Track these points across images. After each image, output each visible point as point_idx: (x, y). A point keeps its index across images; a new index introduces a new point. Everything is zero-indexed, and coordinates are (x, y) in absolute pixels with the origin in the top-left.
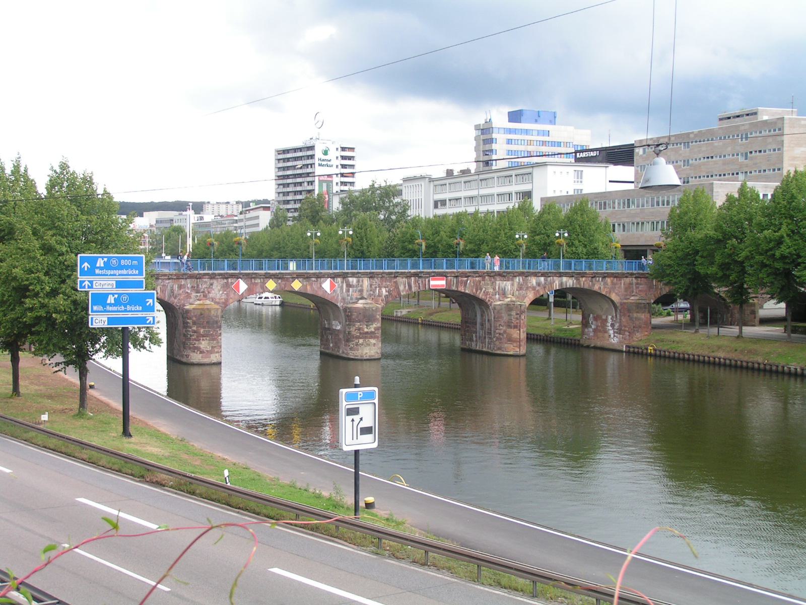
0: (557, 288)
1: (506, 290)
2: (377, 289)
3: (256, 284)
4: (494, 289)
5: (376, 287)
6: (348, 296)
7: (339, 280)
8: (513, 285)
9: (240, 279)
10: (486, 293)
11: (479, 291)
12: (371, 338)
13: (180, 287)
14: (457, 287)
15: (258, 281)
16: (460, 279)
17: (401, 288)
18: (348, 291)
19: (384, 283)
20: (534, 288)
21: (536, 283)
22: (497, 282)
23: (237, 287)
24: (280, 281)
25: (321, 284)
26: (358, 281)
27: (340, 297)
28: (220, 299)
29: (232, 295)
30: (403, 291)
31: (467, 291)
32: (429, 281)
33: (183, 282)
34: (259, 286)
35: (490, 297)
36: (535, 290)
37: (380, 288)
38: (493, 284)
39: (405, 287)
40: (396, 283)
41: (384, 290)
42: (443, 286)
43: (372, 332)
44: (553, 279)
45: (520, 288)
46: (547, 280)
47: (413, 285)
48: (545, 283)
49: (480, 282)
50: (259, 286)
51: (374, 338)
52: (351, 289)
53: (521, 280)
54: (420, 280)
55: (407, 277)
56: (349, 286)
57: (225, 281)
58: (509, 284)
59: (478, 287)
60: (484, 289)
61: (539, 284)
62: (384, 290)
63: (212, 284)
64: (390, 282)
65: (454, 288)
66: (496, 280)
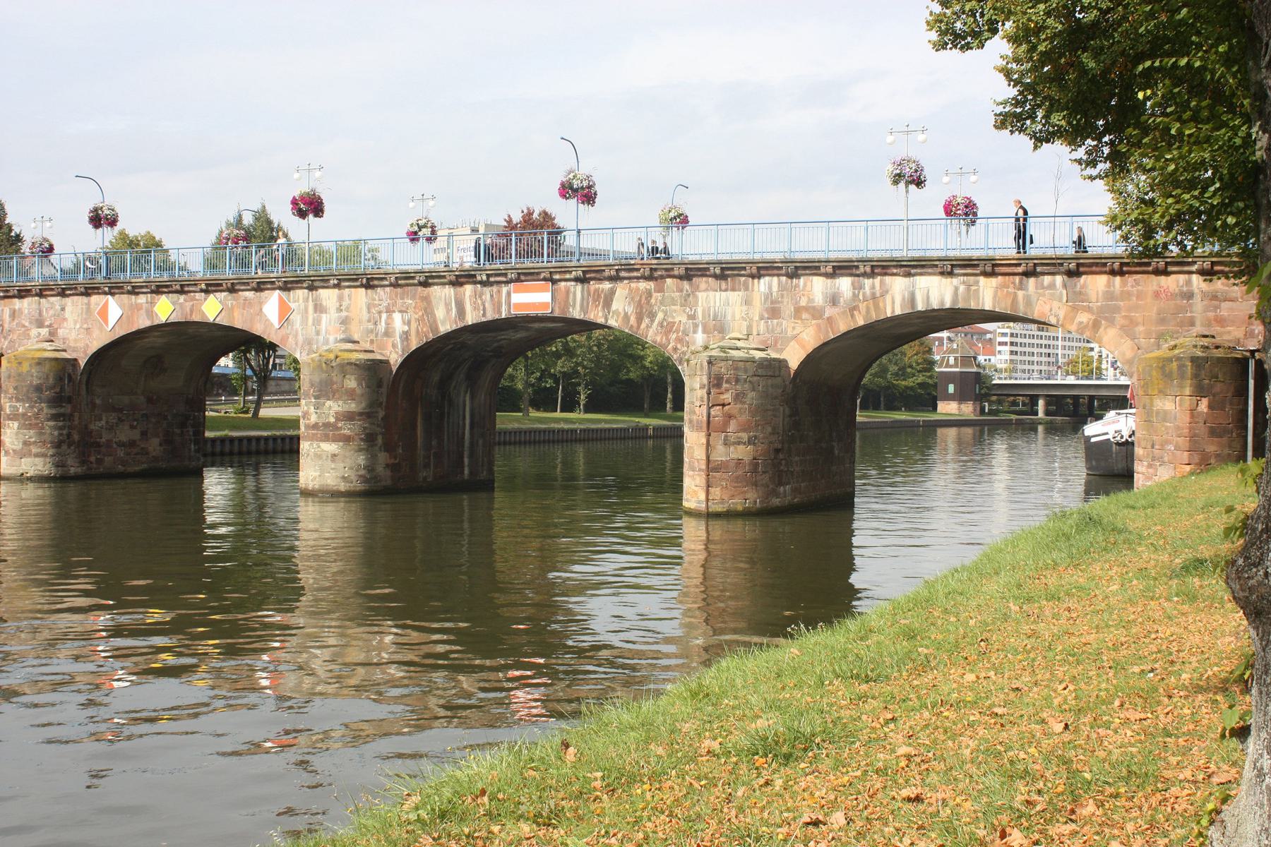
0: (898, 312)
1: (729, 317)
2: (384, 316)
4: (692, 317)
5: (380, 313)
6: (318, 333)
7: (301, 294)
8: (747, 302)
9: (109, 297)
10: (668, 328)
11: (646, 321)
12: (326, 438)
13: (13, 314)
14: (584, 309)
15: (142, 299)
16: (594, 285)
17: (440, 313)
18: (317, 322)
19: (399, 302)
20: (816, 313)
21: (825, 295)
22: (701, 295)
23: (104, 313)
24: (182, 298)
25: (261, 304)
26: (340, 298)
27: (300, 338)
28: (76, 340)
29: (96, 333)
30: (443, 323)
31: (612, 322)
32: (509, 294)
33: (17, 303)
34: (143, 312)
35: (679, 340)
36: (821, 317)
37: (389, 311)
38: (687, 300)
39: (448, 311)
40: (426, 299)
41: (397, 317)
42: (545, 305)
43: (327, 425)
44: (882, 282)
45: (774, 312)
46: (861, 287)
47: (468, 307)
48: (855, 296)
49: (649, 295)
50: (143, 312)
51: (335, 439)
52: (324, 316)
53: (775, 289)
54: (487, 290)
55: (453, 284)
56: (319, 308)
57: (85, 299)
58: (735, 297)
59: (644, 310)
60: (660, 316)
61: (834, 300)
62: (397, 317)
63: (63, 309)
64: (413, 298)
65: (576, 313)
66: (697, 288)
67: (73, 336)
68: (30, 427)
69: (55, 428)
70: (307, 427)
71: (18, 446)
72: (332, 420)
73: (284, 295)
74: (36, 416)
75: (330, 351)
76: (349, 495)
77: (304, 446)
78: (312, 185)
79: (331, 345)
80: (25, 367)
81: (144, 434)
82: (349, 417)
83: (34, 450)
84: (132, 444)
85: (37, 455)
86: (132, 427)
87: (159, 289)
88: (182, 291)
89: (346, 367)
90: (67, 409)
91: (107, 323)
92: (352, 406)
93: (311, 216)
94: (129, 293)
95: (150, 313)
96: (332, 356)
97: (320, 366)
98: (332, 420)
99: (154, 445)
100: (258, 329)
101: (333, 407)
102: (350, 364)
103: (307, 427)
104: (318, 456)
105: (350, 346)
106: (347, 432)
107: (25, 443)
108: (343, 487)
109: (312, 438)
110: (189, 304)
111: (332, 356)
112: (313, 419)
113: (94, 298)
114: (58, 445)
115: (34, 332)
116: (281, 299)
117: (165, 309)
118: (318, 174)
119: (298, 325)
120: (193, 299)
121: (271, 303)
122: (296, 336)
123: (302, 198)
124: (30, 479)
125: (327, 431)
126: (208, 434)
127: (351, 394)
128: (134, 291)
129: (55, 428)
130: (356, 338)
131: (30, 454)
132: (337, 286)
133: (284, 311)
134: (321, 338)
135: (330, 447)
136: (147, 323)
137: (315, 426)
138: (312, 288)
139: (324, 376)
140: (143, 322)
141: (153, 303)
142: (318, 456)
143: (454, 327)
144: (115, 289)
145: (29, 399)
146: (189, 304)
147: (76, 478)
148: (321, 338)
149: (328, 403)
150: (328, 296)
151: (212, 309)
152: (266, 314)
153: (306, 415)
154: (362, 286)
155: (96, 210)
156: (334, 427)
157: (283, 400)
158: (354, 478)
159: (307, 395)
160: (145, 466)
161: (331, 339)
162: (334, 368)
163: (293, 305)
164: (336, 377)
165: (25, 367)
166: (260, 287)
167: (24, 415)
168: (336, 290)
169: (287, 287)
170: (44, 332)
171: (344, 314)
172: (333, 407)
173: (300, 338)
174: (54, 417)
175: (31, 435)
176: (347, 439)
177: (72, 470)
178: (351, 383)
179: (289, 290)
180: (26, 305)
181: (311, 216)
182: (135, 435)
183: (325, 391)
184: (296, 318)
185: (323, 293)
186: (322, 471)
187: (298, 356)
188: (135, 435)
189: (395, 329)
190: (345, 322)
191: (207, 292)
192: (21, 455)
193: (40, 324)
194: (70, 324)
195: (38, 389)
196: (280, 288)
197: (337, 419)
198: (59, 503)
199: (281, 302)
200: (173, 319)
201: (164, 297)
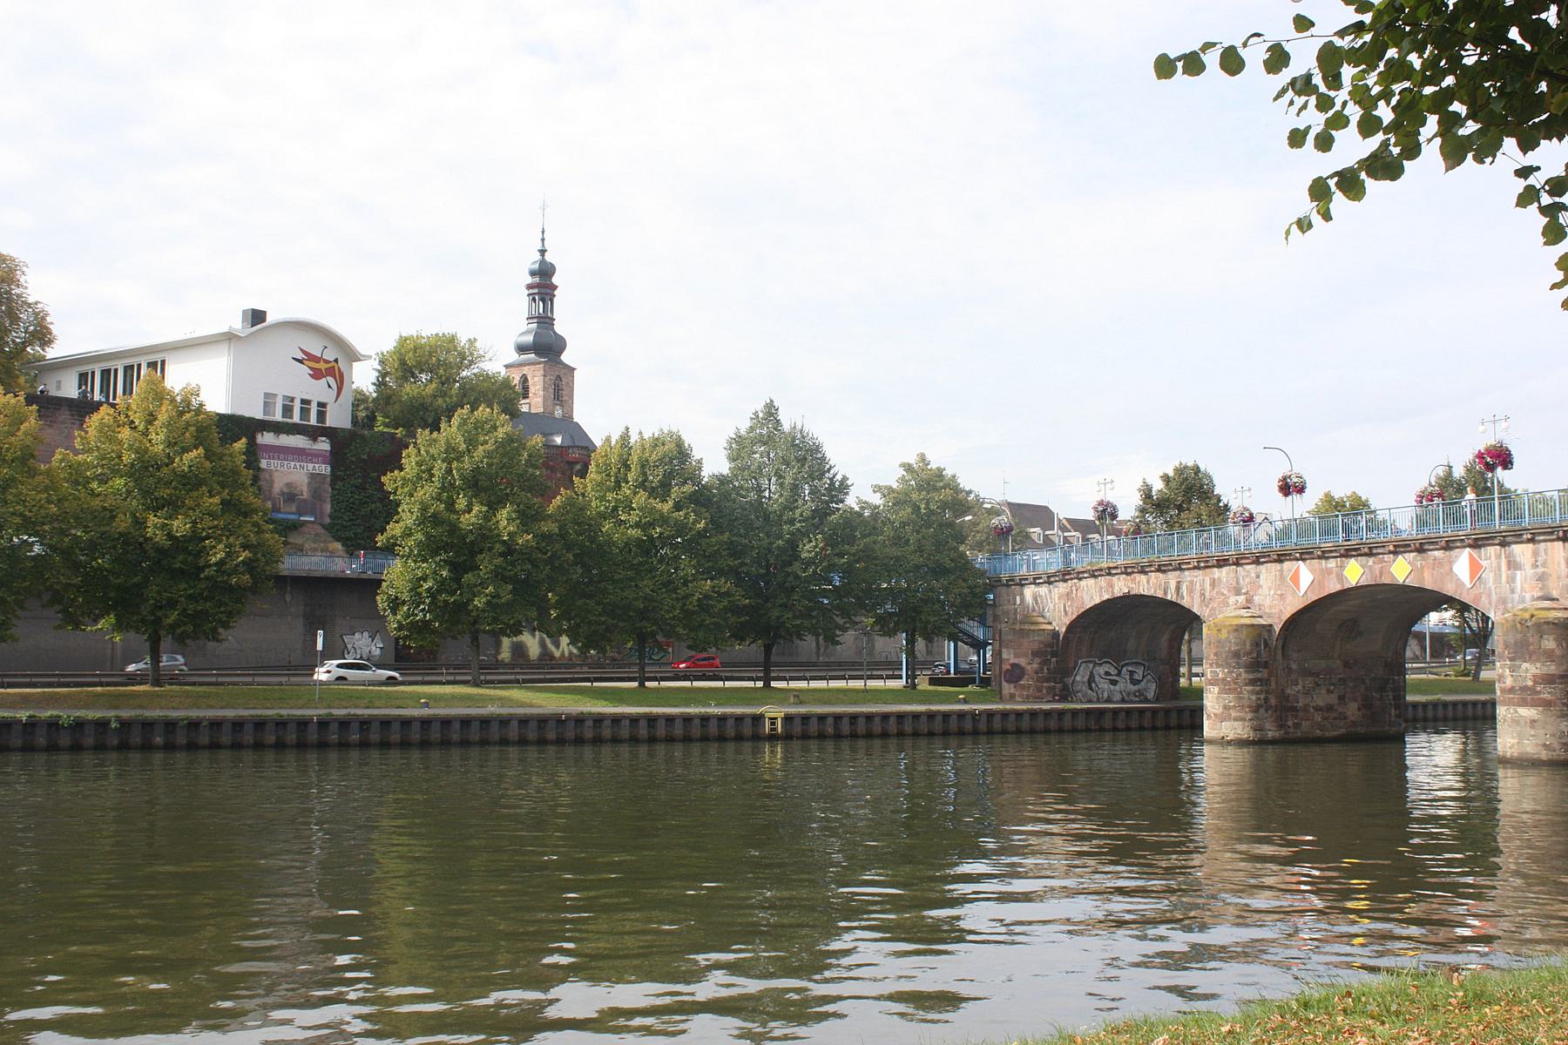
3: (1329, 571)
6: (1513, 591)
7: (1492, 551)
12: (1523, 703)
13: (1213, 583)
15: (1332, 563)
18: (1511, 580)
23: (1296, 578)
24: (1371, 561)
25: (1451, 563)
26: (1536, 554)
27: (1494, 597)
29: (1289, 598)
34: (1333, 576)
43: (1524, 689)
50: (1333, 576)
56: (1513, 565)
57: (1278, 566)
67: (1268, 602)
68: (1230, 691)
69: (1252, 692)
70: (1503, 691)
71: (1219, 710)
72: (1530, 683)
73: (1474, 553)
74: (1235, 681)
75: (1524, 610)
76: (1552, 764)
77: (1501, 711)
78: (1499, 437)
79: (1528, 604)
80: (1224, 635)
81: (1342, 698)
82: (1549, 680)
83: (1234, 714)
84: (1330, 708)
85: (1236, 719)
86: (1329, 691)
87: (1347, 554)
88: (1370, 554)
89: (1543, 627)
90: (1264, 674)
91: (1298, 586)
92: (1552, 669)
93: (1499, 469)
94: (1319, 558)
95: (1341, 577)
96: (1527, 616)
97: (1514, 626)
98: (1530, 683)
99: (1352, 710)
100: (1449, 589)
101: (1530, 670)
102: (1548, 623)
103: (1503, 691)
104: (1516, 722)
105: (1547, 604)
106: (1546, 696)
107: (1225, 707)
108: (1544, 755)
109: (1510, 703)
110: (1378, 567)
111: (1527, 616)
112: (1509, 682)
113: (1286, 564)
114: (1256, 709)
115: (1232, 600)
116: (1471, 556)
117: (1354, 573)
118: (1504, 424)
119: (1491, 584)
120: (1383, 561)
121: (1461, 562)
122: (1489, 595)
123: (1489, 451)
124: (1229, 743)
125: (1525, 695)
126: (1409, 698)
127: (1549, 655)
128: (1324, 556)
129: (1252, 692)
130: (1555, 594)
131: (1229, 718)
132: (1532, 540)
133: (1475, 567)
134: (1516, 596)
135: (1527, 712)
136: (1338, 588)
137: (1511, 690)
138: (1503, 544)
139: (1519, 636)
140: (1333, 587)
141: (1342, 567)
142: (1516, 722)
143: (1151, 593)
144: (1305, 555)
145: (1228, 665)
146: (1378, 567)
147: (1273, 742)
148: (1516, 596)
149: (1525, 665)
150: (1522, 551)
151: (1401, 570)
152: (1459, 571)
153: (1501, 678)
154: (1559, 539)
155: (1284, 479)
156: (1532, 690)
157: (525, 681)
158: (1556, 746)
159: (1502, 658)
160: (1343, 731)
161: (1528, 596)
162: (1530, 631)
163: (1484, 563)
164: (1532, 638)
165: (1224, 635)
166: (1448, 547)
167: (1224, 680)
168: (1531, 545)
169: (1477, 544)
170: (1241, 599)
171: (1540, 570)
172: (1530, 670)
173: (1494, 597)
174: (1252, 682)
175: (1230, 699)
176: (1547, 704)
177: (1270, 734)
178: (1549, 643)
179: (1479, 547)
180: (1223, 574)
181: (1499, 469)
182: (1333, 699)
183: (1521, 651)
184: (1489, 576)
185: (1517, 549)
186: (1521, 737)
187: (1492, 615)
188: (1333, 699)
189: (1281, 593)
190: (1541, 578)
191: (1395, 553)
192: (1222, 718)
193: (1238, 592)
194: (1264, 590)
195: (1236, 655)
196: (1470, 546)
197: (1535, 682)
198: (1258, 767)
199: (1472, 561)
200: (1363, 582)
201: (1353, 560)
